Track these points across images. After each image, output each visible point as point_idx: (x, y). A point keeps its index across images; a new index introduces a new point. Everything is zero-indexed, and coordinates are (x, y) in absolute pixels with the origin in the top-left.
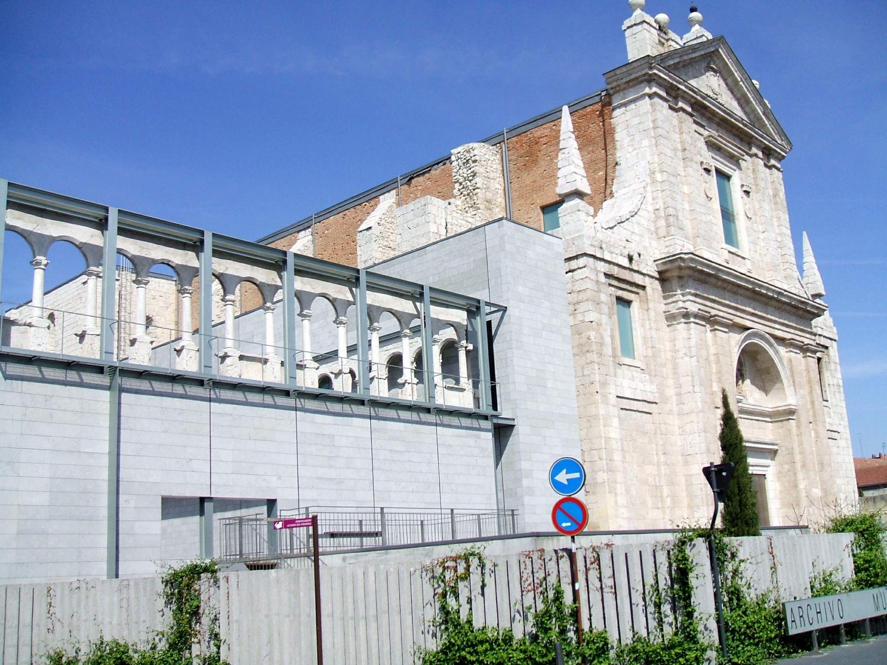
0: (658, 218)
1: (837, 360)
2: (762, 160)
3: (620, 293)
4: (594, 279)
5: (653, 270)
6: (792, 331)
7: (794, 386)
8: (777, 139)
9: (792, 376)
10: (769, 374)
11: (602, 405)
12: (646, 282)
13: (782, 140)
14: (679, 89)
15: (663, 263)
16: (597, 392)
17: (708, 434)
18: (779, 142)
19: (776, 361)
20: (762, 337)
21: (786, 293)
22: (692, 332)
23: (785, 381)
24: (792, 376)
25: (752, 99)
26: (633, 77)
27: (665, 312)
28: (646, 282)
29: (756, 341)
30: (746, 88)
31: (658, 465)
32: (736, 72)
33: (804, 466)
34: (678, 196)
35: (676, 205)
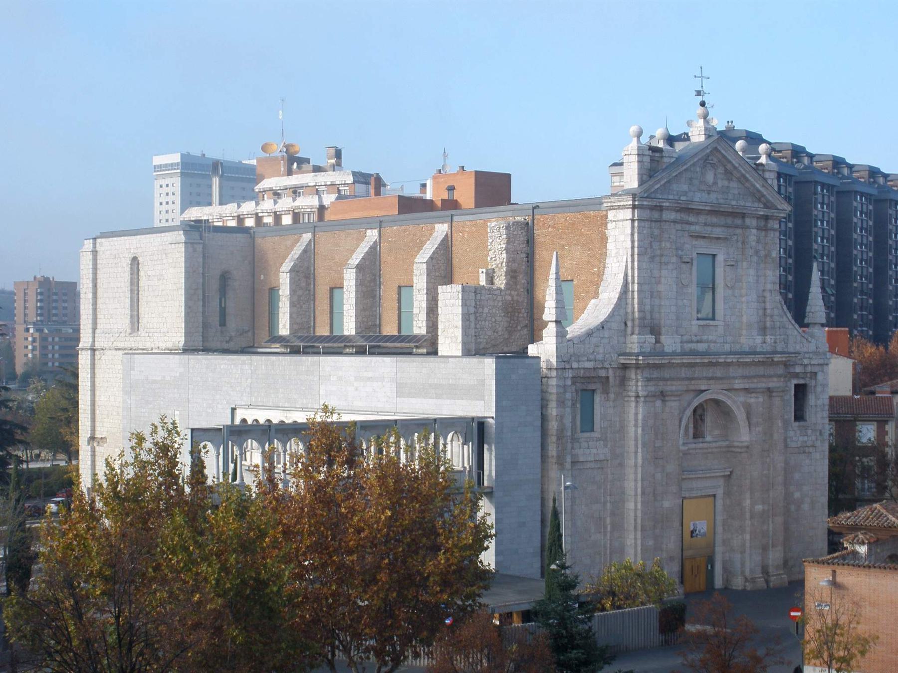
18: (779, 207)
19: (734, 408)
20: (717, 393)
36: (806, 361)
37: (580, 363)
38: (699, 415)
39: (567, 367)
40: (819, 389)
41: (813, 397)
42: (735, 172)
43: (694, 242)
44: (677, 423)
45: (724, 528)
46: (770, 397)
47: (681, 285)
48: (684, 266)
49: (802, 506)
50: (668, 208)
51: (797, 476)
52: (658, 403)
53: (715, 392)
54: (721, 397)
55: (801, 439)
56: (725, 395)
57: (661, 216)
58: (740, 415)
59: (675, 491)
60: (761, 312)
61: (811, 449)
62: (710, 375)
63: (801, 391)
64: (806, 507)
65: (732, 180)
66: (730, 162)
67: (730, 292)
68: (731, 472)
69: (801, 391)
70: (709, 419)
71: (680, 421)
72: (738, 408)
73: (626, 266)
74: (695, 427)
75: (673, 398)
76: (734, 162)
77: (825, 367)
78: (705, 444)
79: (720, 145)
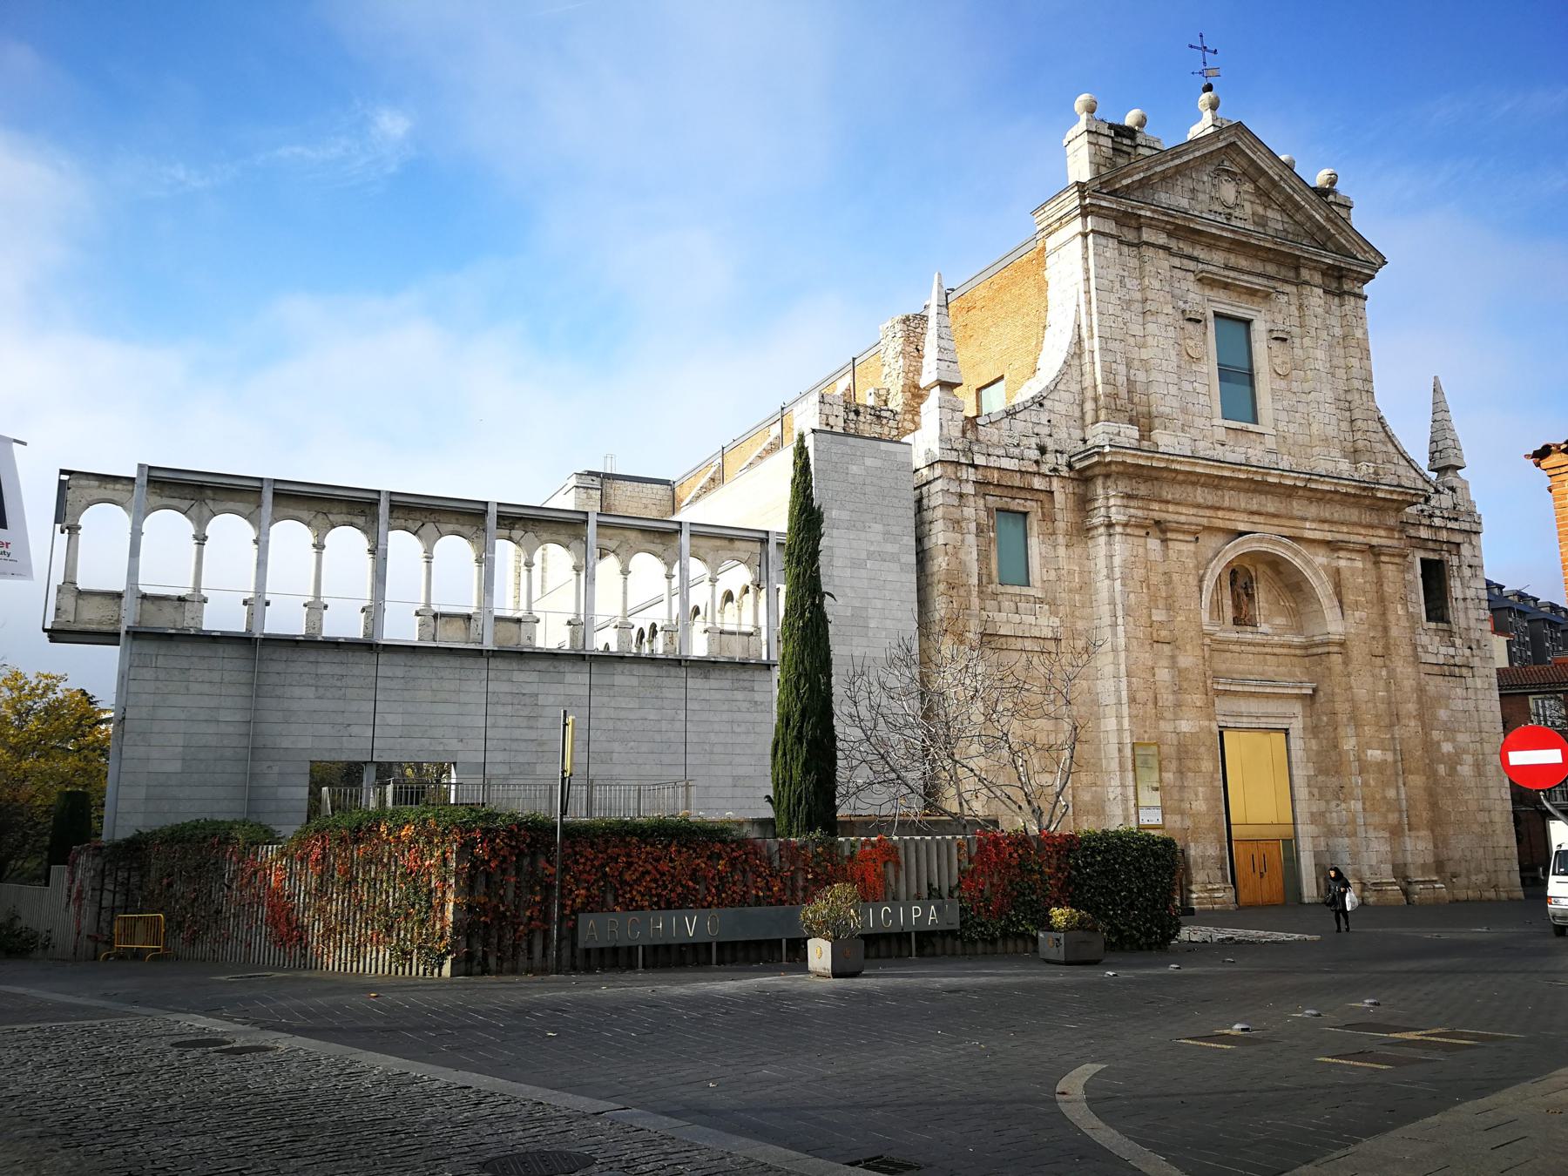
7: (1341, 607)
10: (1301, 590)
13: (1365, 252)
14: (1140, 216)
17: (1134, 679)
18: (1359, 256)
19: (1308, 573)
21: (1322, 479)
22: (1117, 547)
23: (1325, 601)
29: (1265, 547)
30: (1291, 187)
36: (1437, 522)
38: (1240, 581)
39: (963, 460)
40: (1467, 572)
41: (1458, 583)
42: (1274, 194)
43: (1208, 292)
44: (1193, 581)
45: (1310, 792)
46: (1377, 563)
47: (1187, 358)
48: (1190, 326)
49: (1459, 767)
50: (1152, 224)
51: (1443, 714)
52: (1154, 544)
53: (1264, 539)
54: (1280, 551)
55: (1443, 650)
56: (1288, 548)
57: (1140, 237)
58: (1322, 588)
59: (1198, 704)
60: (1345, 426)
61: (1464, 671)
62: (1255, 507)
63: (1435, 577)
64: (1465, 770)
65: (1270, 206)
66: (1263, 173)
67: (1283, 384)
68: (1315, 690)
69: (1435, 577)
70: (1262, 596)
71: (1201, 580)
72: (1316, 573)
73: (1078, 312)
74: (1237, 607)
75: (1181, 537)
76: (1270, 172)
77: (1473, 536)
78: (1259, 636)
79: (1240, 139)
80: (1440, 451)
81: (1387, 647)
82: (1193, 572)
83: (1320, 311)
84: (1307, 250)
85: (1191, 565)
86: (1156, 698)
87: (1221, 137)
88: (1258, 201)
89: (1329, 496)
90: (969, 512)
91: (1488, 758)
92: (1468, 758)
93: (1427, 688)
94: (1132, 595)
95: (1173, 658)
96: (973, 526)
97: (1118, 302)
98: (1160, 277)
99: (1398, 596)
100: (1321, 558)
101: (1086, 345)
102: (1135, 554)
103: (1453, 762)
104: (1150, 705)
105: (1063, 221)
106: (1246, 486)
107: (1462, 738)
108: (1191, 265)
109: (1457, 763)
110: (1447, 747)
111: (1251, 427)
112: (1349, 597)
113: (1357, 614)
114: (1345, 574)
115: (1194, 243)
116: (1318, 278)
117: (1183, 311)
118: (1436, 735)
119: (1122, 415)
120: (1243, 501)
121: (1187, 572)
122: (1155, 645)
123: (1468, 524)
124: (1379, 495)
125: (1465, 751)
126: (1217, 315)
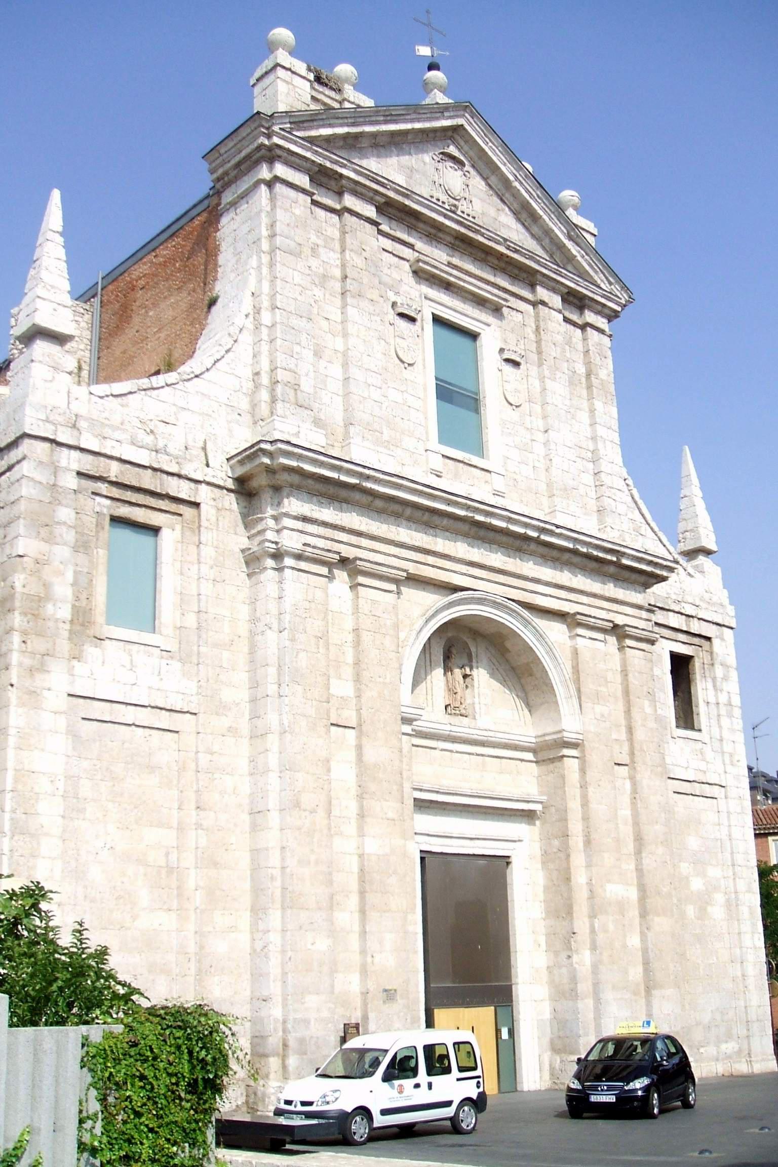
0: (257, 386)
1: (732, 661)
2: (560, 312)
3: (124, 511)
4: (44, 482)
5: (223, 474)
6: (585, 599)
7: (580, 698)
8: (599, 282)
9: (577, 681)
10: (531, 675)
11: (20, 710)
12: (204, 494)
13: (610, 283)
14: (341, 176)
15: (239, 461)
16: (12, 685)
18: (602, 286)
19: (540, 652)
20: (496, 605)
21: (558, 531)
23: (559, 689)
24: (577, 681)
25: (541, 212)
26: (243, 154)
27: (243, 551)
28: (204, 494)
30: (527, 191)
31: (181, 829)
32: (505, 165)
33: (588, 842)
34: (305, 352)
35: (296, 365)
37: (109, 443)
48: (403, 324)
49: (709, 909)
50: (358, 191)
51: (693, 843)
59: (391, 815)
64: (717, 912)
65: (503, 210)
79: (470, 124)
80: (691, 531)
81: (632, 754)
82: (391, 632)
83: (559, 338)
84: (546, 267)
85: (389, 623)
86: (330, 803)
87: (446, 114)
88: (488, 201)
89: (567, 556)
90: (65, 514)
91: (741, 896)
92: (719, 898)
93: (676, 809)
94: (302, 655)
95: (359, 748)
96: (70, 536)
97: (307, 272)
98: (364, 254)
99: (645, 689)
100: (556, 631)
101: (266, 318)
102: (310, 598)
103: (703, 902)
104: (321, 813)
105: (242, 167)
106: (465, 527)
107: (714, 872)
108: (406, 252)
109: (707, 903)
110: (697, 884)
111: (475, 460)
112: (588, 686)
113: (599, 709)
114: (585, 656)
115: (411, 228)
116: (556, 300)
117: (394, 305)
118: (685, 868)
119: (307, 412)
120: (461, 549)
121: (383, 631)
122: (333, 728)
123: (720, 616)
124: (625, 561)
125: (716, 889)
126: (438, 320)
